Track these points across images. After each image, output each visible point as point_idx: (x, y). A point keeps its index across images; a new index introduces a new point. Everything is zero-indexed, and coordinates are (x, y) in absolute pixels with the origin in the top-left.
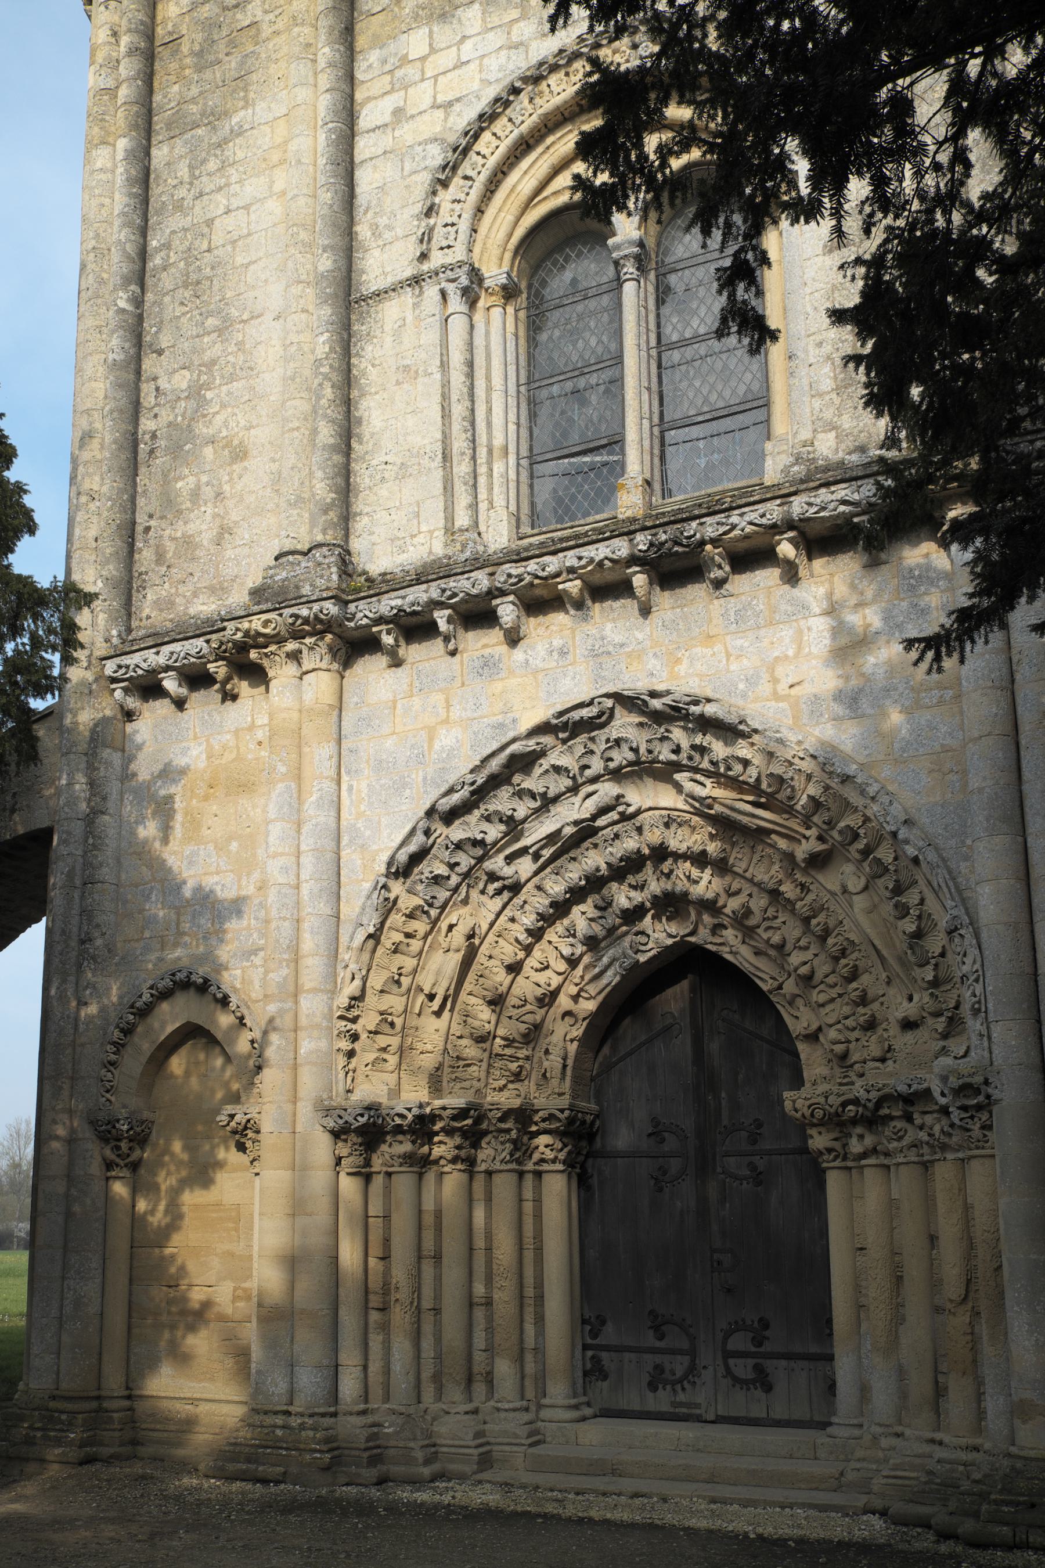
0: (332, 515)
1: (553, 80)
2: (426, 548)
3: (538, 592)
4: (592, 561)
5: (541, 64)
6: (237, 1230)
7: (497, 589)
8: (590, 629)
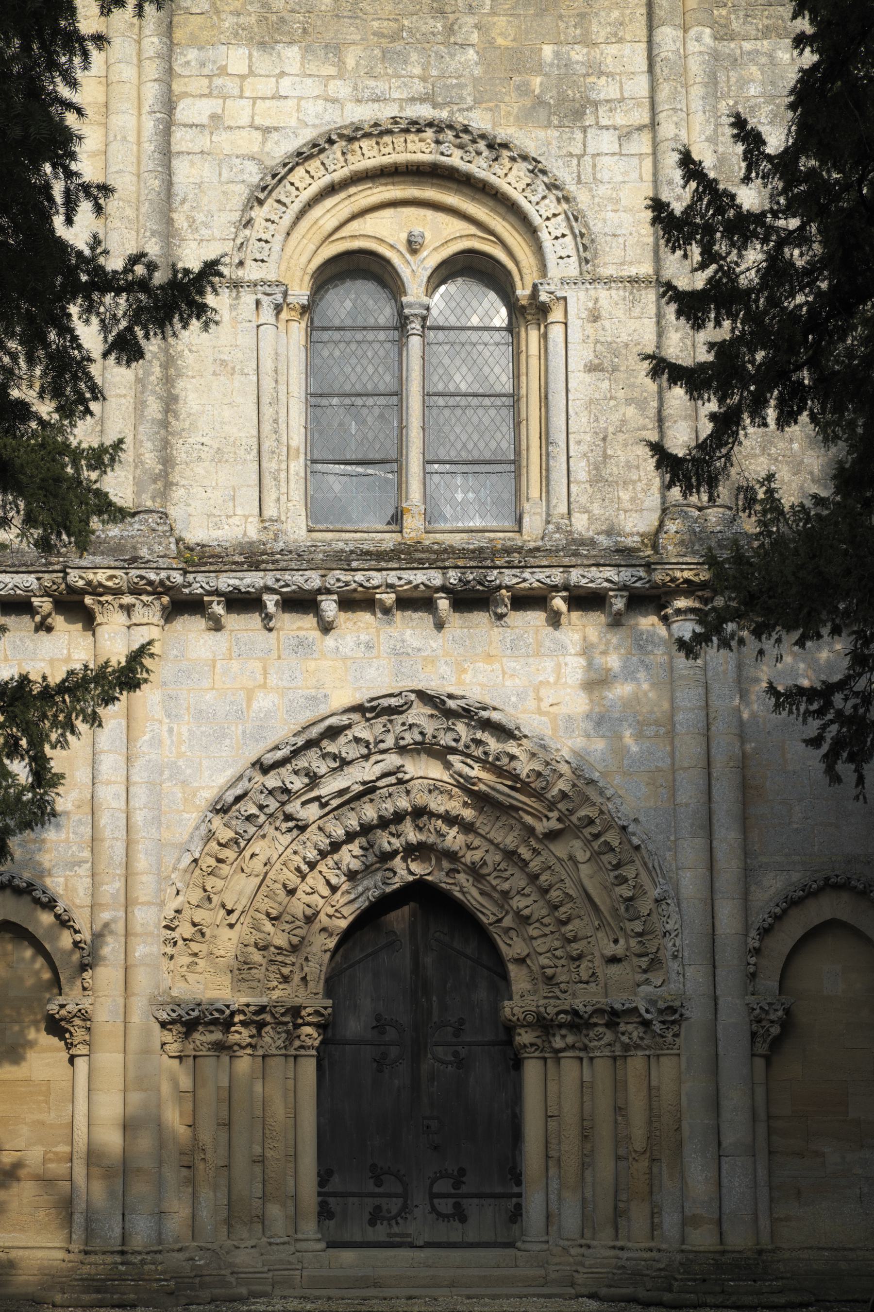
0: (160, 484)
1: (365, 143)
2: (242, 528)
4: (410, 582)
6: (47, 1102)
7: (326, 588)
8: (390, 630)
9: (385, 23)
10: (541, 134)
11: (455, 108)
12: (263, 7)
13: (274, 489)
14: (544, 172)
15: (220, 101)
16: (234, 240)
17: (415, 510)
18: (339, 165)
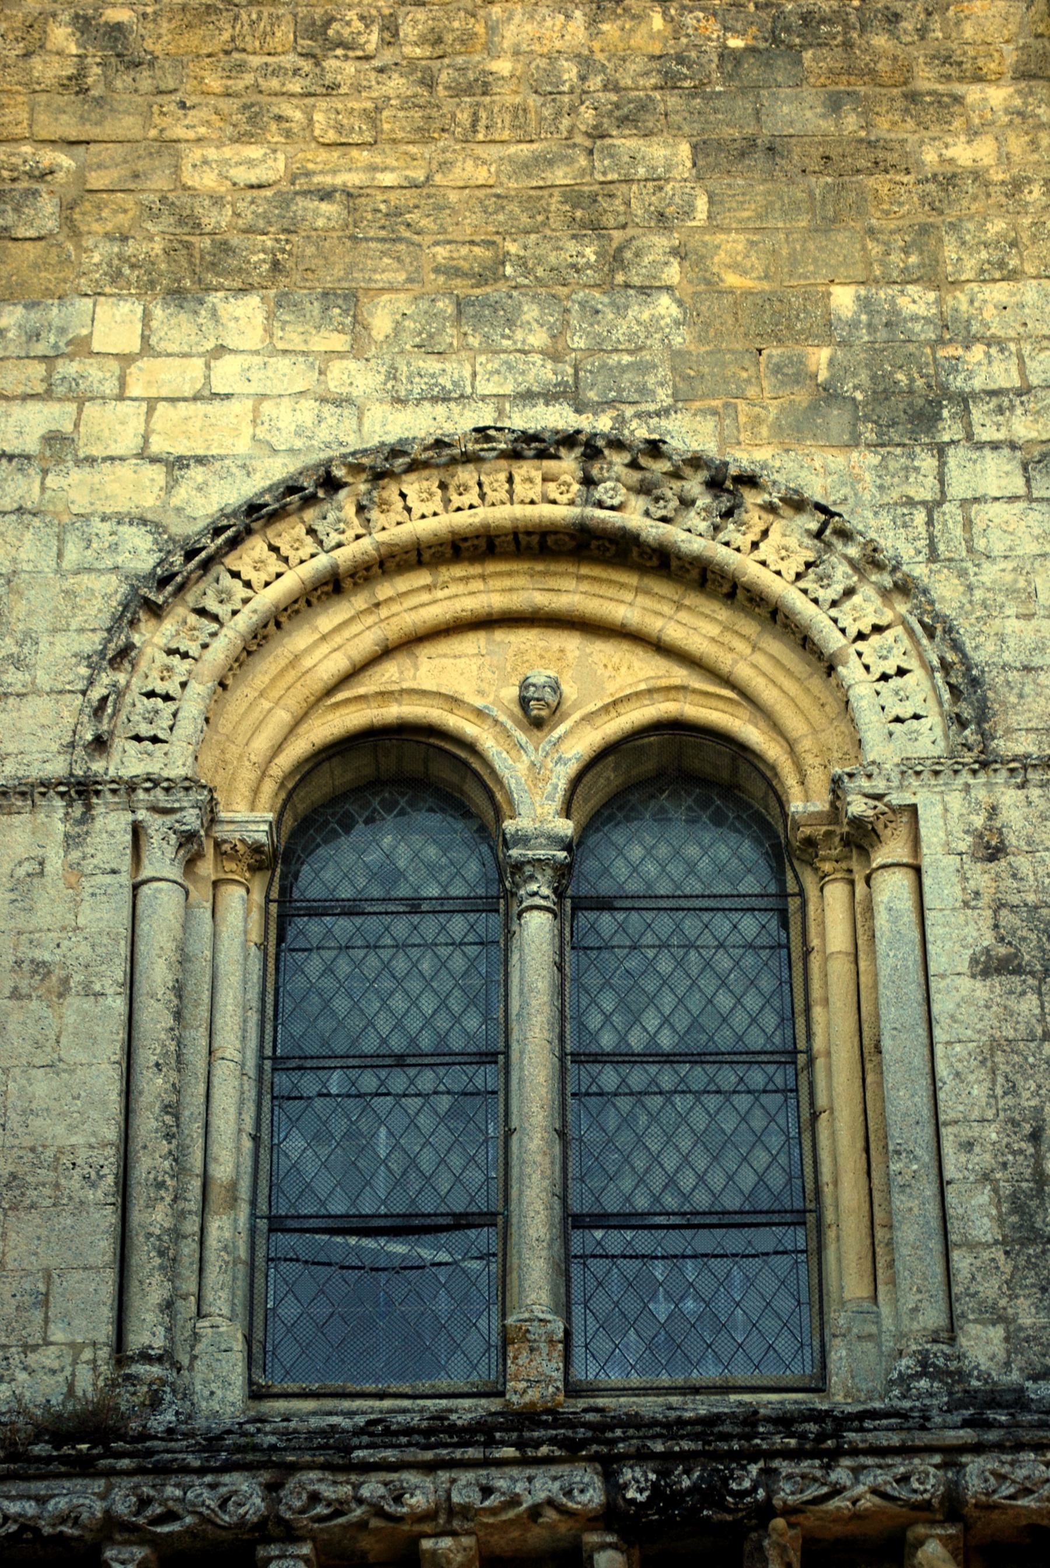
1: (413, 486)
3: (366, 1543)
4: (514, 1501)
5: (395, 452)
9: (464, 250)
10: (837, 460)
11: (629, 411)
12: (181, 221)
13: (158, 1277)
14: (845, 535)
15: (72, 407)
16: (84, 693)
17: (537, 1331)
18: (351, 534)
